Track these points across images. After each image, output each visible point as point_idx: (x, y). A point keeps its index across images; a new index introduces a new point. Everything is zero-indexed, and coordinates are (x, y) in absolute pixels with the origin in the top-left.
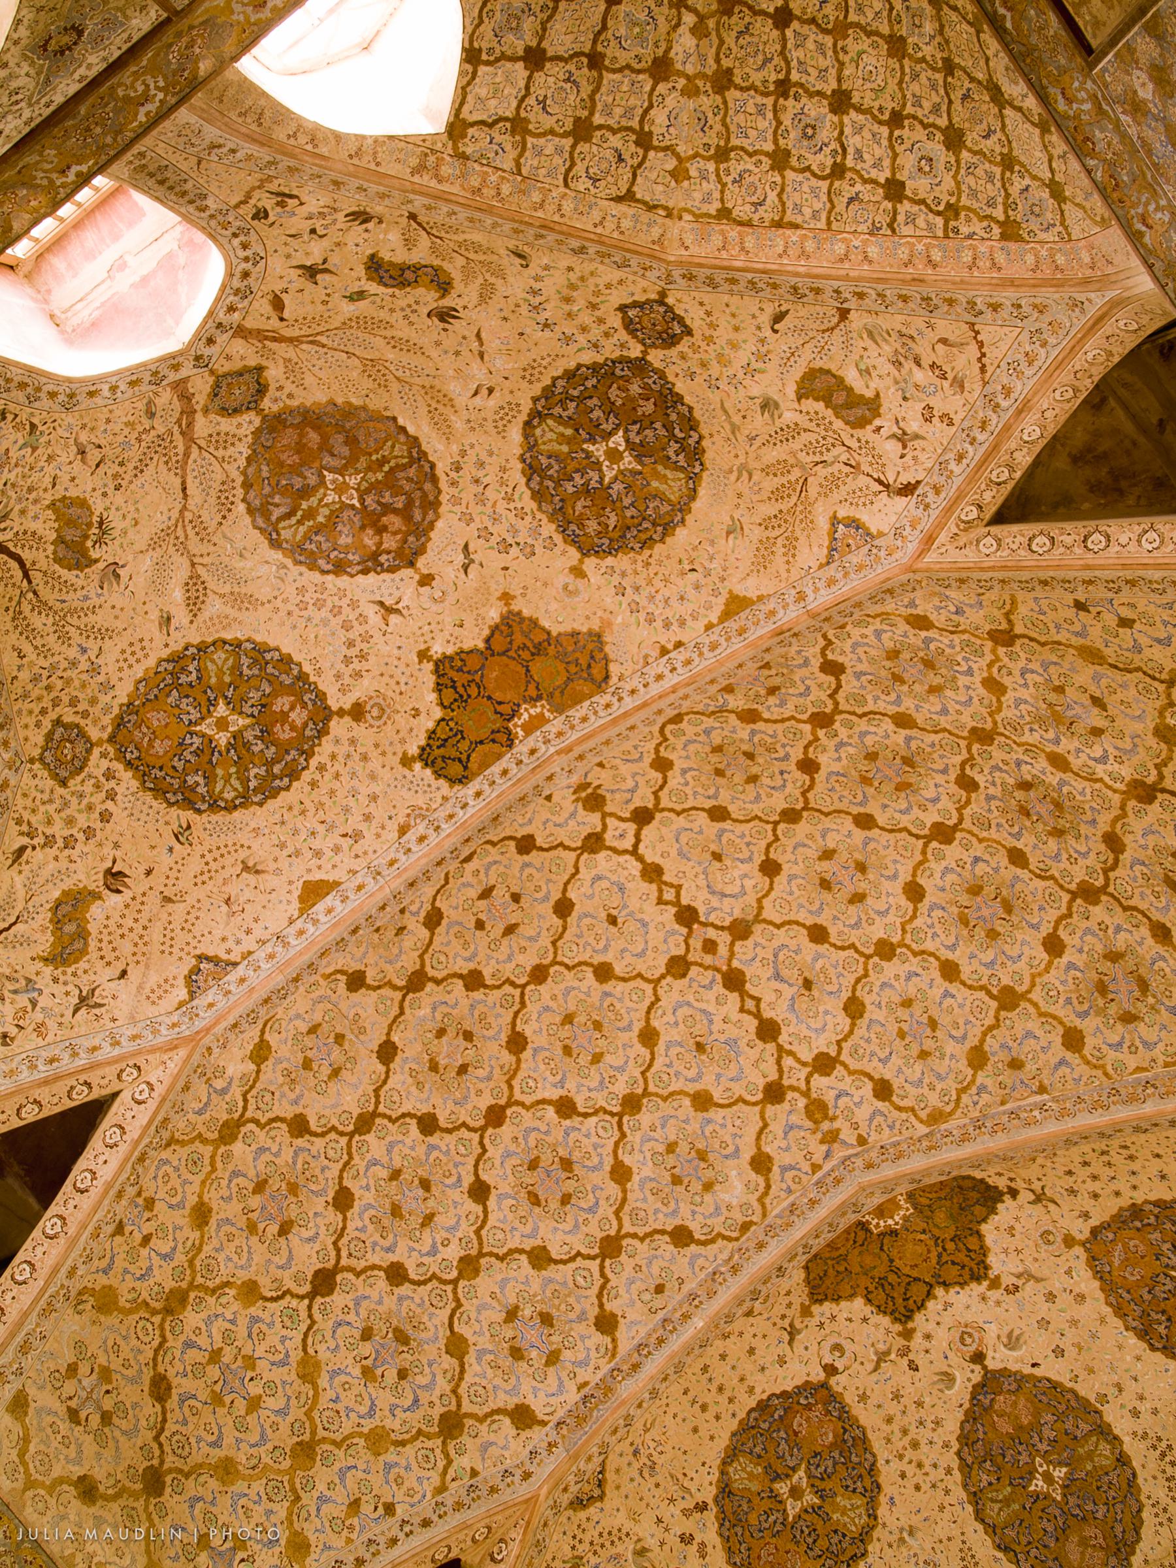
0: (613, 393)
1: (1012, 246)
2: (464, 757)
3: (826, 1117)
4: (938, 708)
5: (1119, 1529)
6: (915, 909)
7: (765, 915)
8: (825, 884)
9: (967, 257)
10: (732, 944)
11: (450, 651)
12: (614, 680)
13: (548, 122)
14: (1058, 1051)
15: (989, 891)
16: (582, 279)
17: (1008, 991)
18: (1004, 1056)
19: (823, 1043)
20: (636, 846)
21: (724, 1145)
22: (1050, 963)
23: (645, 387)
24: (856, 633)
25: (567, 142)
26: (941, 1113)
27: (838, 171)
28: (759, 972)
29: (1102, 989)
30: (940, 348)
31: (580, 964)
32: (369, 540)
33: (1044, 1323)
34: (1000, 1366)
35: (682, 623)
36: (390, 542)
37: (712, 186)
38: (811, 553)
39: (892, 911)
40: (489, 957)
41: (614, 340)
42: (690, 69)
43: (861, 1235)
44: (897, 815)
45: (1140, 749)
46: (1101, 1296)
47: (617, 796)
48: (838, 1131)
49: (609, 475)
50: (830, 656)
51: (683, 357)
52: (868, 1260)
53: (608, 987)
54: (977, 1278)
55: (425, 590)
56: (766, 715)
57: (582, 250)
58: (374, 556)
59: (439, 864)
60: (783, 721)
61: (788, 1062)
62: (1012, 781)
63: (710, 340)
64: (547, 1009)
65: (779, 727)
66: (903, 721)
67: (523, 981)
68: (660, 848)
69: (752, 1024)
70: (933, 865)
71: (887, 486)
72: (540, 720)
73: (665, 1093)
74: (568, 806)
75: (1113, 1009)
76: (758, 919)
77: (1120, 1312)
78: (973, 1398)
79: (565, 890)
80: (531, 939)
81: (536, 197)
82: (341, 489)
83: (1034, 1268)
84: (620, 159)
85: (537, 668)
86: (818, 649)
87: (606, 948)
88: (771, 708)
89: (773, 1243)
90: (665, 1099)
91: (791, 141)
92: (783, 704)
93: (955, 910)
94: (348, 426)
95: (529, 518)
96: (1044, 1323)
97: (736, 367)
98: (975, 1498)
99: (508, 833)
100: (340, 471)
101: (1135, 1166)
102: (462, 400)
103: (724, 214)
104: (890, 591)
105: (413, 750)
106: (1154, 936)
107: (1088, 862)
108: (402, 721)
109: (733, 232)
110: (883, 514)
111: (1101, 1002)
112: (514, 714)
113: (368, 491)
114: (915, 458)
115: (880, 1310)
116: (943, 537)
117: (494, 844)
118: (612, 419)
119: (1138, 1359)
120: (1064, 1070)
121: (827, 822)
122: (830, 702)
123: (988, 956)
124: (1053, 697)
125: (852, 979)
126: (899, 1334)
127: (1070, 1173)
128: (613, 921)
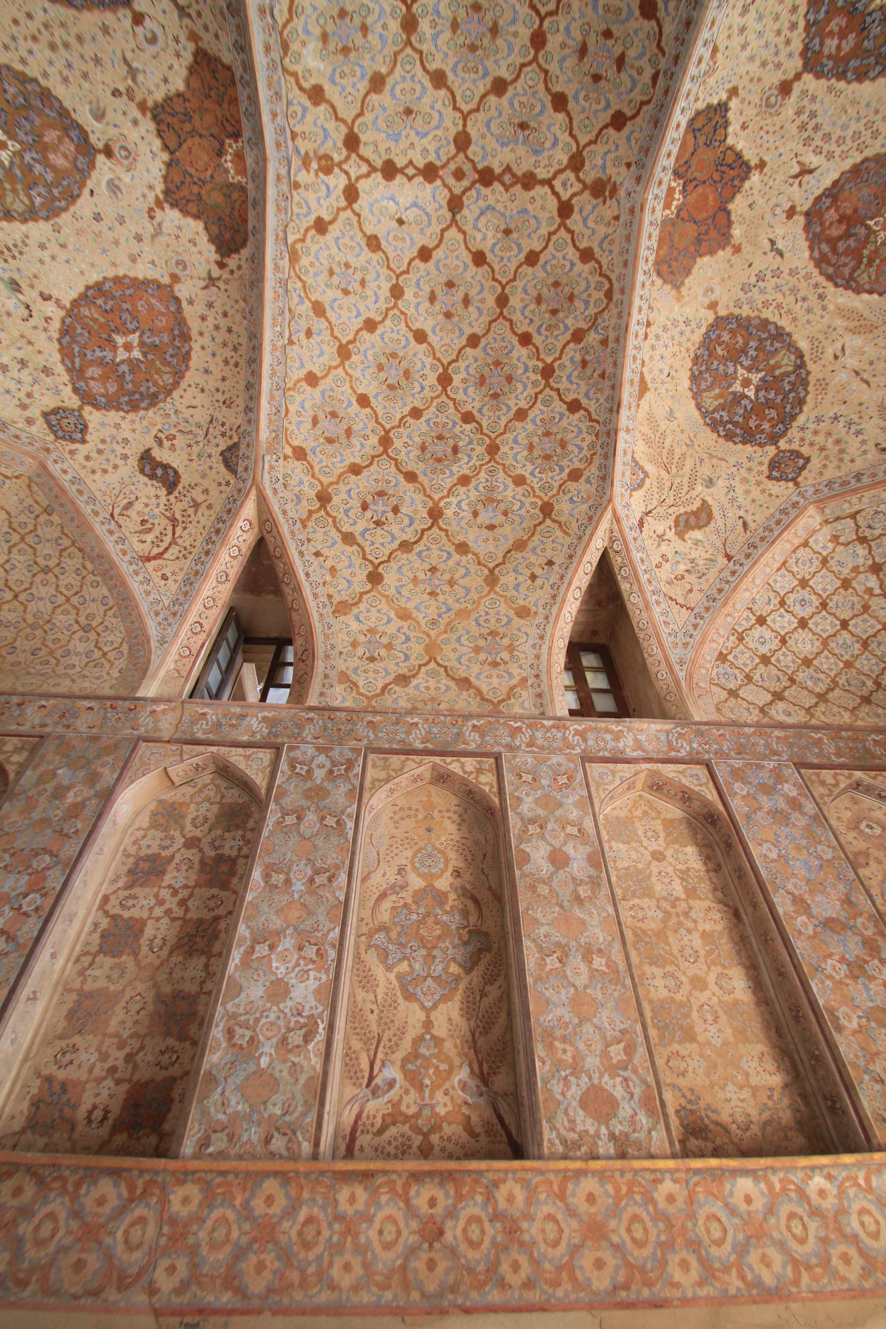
0: (773, 413)
1: (716, 654)
2: (698, 134)
4: (519, 439)
7: (454, 229)
8: (450, 284)
9: (722, 632)
10: (450, 191)
11: (747, 185)
12: (654, 277)
14: (309, 367)
15: (404, 383)
16: (841, 460)
18: (314, 330)
20: (552, 188)
21: (343, 75)
23: (762, 432)
24: (589, 438)
27: (782, 603)
29: (334, 415)
30: (689, 587)
31: (518, 76)
33: (121, 220)
35: (653, 348)
37: (817, 548)
40: (582, 16)
41: (797, 440)
42: (862, 576)
43: (230, 129)
46: (132, 274)
47: (589, 207)
48: (308, 171)
49: (741, 371)
50: (582, 412)
51: (761, 463)
53: (488, 81)
54: (167, 192)
55: (787, 206)
56: (572, 345)
59: (677, 58)
61: (365, 169)
62: (461, 444)
64: (514, 21)
65: (559, 346)
66: (521, 415)
67: (546, 24)
68: (539, 202)
69: (400, 162)
72: (667, 206)
73: (399, 58)
74: (611, 171)
75: (321, 415)
76: (454, 221)
77: (117, 280)
78: (80, 127)
79: (568, 114)
80: (564, 59)
83: (163, 239)
84: (869, 527)
85: (691, 230)
86: (592, 410)
87: (512, 104)
88: (573, 352)
89: (265, 63)
90: (396, 54)
91: (805, 593)
92: (572, 359)
93: (401, 354)
95: (760, 306)
99: (638, 120)
101: (219, 359)
103: (806, 544)
104: (603, 478)
105: (734, 104)
108: (751, 112)
109: (797, 542)
111: (328, 410)
112: (684, 191)
113: (868, 236)
115: (168, 99)
116: (615, 527)
117: (643, 103)
118: (763, 400)
119: (82, 273)
120: (298, 364)
121: (485, 319)
122: (555, 386)
123: (371, 358)
124: (502, 506)
125: (391, 256)
127: (225, 315)
128: (523, 126)
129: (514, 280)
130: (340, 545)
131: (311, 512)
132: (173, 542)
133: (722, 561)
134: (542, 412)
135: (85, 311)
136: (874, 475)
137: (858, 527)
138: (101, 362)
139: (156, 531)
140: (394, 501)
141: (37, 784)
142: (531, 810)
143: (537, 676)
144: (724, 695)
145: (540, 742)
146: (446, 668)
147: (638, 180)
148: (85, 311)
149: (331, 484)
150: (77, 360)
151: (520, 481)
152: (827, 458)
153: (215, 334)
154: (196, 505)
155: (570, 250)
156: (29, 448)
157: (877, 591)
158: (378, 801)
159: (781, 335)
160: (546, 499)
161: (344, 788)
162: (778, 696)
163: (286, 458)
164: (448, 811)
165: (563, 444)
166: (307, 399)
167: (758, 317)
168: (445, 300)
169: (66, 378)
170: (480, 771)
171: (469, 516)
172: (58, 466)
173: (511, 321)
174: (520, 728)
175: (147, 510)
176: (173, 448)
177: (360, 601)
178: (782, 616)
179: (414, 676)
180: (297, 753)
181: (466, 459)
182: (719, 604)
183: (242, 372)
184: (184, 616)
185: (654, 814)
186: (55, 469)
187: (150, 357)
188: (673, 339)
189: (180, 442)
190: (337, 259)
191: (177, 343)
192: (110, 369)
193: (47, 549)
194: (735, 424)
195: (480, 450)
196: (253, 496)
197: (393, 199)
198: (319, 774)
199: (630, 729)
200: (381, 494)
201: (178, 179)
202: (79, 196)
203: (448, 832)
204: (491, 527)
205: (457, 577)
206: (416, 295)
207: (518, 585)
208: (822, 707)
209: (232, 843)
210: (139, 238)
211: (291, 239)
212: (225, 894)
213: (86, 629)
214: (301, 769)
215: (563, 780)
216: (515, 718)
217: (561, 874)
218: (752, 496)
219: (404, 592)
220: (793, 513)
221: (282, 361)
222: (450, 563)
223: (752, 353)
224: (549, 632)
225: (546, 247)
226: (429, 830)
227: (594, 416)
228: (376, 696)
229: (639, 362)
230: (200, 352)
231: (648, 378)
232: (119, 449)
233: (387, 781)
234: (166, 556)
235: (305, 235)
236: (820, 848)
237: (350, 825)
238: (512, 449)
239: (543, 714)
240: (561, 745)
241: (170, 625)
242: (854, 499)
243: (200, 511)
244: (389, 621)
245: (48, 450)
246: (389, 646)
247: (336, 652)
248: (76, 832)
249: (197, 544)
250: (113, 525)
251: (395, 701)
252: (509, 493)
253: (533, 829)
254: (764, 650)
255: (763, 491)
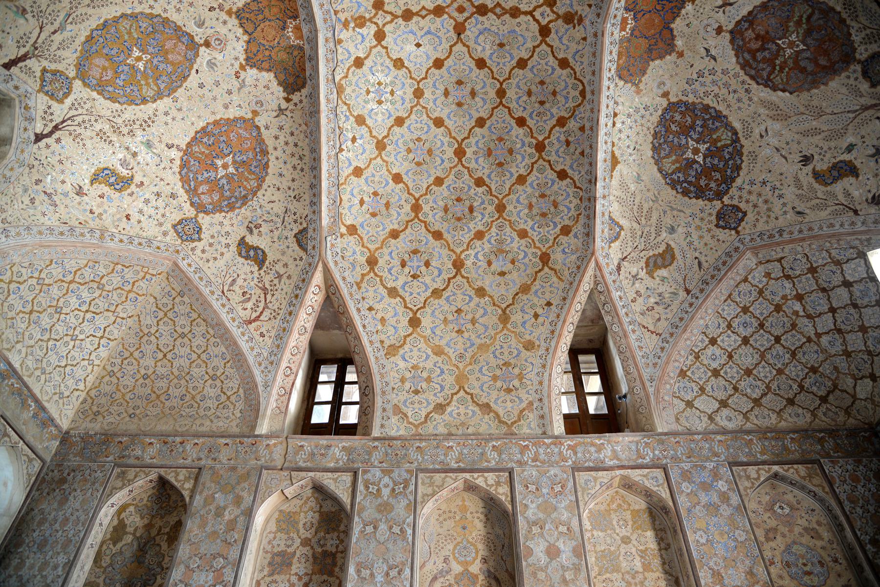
0: (718, 176)
1: (678, 371)
3: (356, 26)
5: (111, 89)
6: (431, 119)
7: (460, 45)
8: (459, 83)
9: (682, 353)
10: (455, 20)
11: (683, 11)
13: (827, 268)
15: (427, 159)
16: (769, 216)
17: (384, 148)
19: (388, 41)
20: (533, 17)
22: (390, 173)
23: (710, 189)
25: (815, 265)
26: (342, 92)
27: (729, 326)
28: (435, 25)
29: (375, 194)
30: (657, 316)
32: (760, 30)
33: (217, 84)
34: (200, 54)
36: (749, 34)
37: (755, 282)
38: (616, 209)
39: (434, 107)
41: (736, 197)
42: (790, 302)
43: (291, 14)
44: (477, 139)
45: (476, 276)
46: (226, 117)
47: (563, 30)
48: (348, 30)
49: (691, 142)
51: (710, 214)
52: (275, 10)
55: (716, 26)
56: (557, 128)
57: (781, 232)
58: (751, 23)
60: (550, 132)
61: (389, 18)
62: (475, 204)
63: (709, 230)
65: (548, 128)
66: (521, 180)
68: (524, 26)
69: (415, 9)
70: (447, 139)
71: (623, 260)
72: (623, 29)
74: (576, 7)
77: (216, 123)
81: (814, 246)
82: (792, 44)
83: (246, 90)
84: (791, 268)
86: (576, 179)
91: (747, 317)
92: (558, 138)
93: (424, 137)
94: (810, 77)
95: (702, 95)
96: (217, 84)
97: (692, 230)
98: (134, 16)
100: (798, 53)
101: (289, 166)
102: (769, 122)
103: (745, 280)
104: (588, 235)
106: (393, 230)
107: (430, 216)
109: (738, 278)
110: (615, 252)
113: (778, 51)
114: (627, 278)
119: (193, 124)
122: (547, 158)
125: (412, 69)
126: (231, 9)
127: (292, 134)
129: (509, 78)
130: (387, 300)
131: (363, 275)
132: (266, 307)
133: (682, 294)
134: (538, 178)
135: (196, 149)
136: (791, 233)
137: (784, 268)
138: (208, 181)
139: (253, 300)
140: (425, 257)
141: (204, 506)
142: (534, 514)
143: (540, 400)
144: (683, 405)
145: (542, 457)
146: (472, 395)
147: (598, 15)
148: (196, 149)
149: (377, 249)
150: (192, 183)
151: (523, 234)
152: (758, 213)
153: (285, 148)
154: (280, 277)
155: (551, 58)
156: (167, 254)
157: (802, 313)
158: (427, 509)
159: (720, 117)
160: (544, 250)
161: (404, 503)
162: (724, 404)
163: (342, 235)
164: (477, 512)
165: (555, 205)
166: (356, 187)
167: (701, 103)
168: (457, 94)
169: (185, 197)
170: (498, 484)
171: (485, 265)
172: (185, 262)
173: (509, 108)
174: (527, 446)
175: (245, 284)
176: (260, 234)
177: (405, 343)
178: (729, 336)
179: (448, 404)
180: (369, 476)
181: (480, 217)
182: (680, 330)
183: (307, 176)
184: (278, 365)
185: (626, 506)
186: (183, 265)
187: (240, 170)
188: (636, 121)
189: (264, 229)
190: (372, 81)
191: (258, 157)
192: (214, 185)
193: (182, 321)
194: (690, 183)
195: (491, 209)
196: (320, 268)
197: (412, 32)
198: (386, 492)
199: (609, 442)
200: (415, 252)
201: (255, 50)
202: (188, 75)
203: (477, 528)
204: (502, 274)
205: (477, 316)
206: (433, 93)
207: (525, 323)
208: (756, 411)
209: (332, 542)
210: (230, 92)
211: (337, 80)
212: (331, 579)
213: (213, 378)
214: (373, 489)
215: (558, 488)
216: (524, 439)
217: (554, 564)
218: (704, 241)
219: (438, 332)
220: (736, 256)
221: (337, 165)
222: (472, 304)
223: (699, 129)
224: (549, 362)
225: (532, 56)
226: (464, 528)
227: (578, 184)
228: (422, 423)
229: (610, 144)
230: (276, 162)
231: (617, 153)
232: (224, 241)
233: (433, 495)
234: (262, 318)
235: (347, 73)
236: (737, 532)
237: (410, 532)
238: (515, 207)
239: (544, 433)
240: (557, 459)
241: (269, 372)
242: (778, 249)
243: (283, 281)
244: (428, 357)
245: (178, 252)
246: (429, 380)
247: (389, 388)
248: (235, 541)
249: (283, 307)
250: (224, 300)
251: (435, 427)
252: (515, 245)
253: (535, 530)
254: (715, 365)
255: (713, 237)
